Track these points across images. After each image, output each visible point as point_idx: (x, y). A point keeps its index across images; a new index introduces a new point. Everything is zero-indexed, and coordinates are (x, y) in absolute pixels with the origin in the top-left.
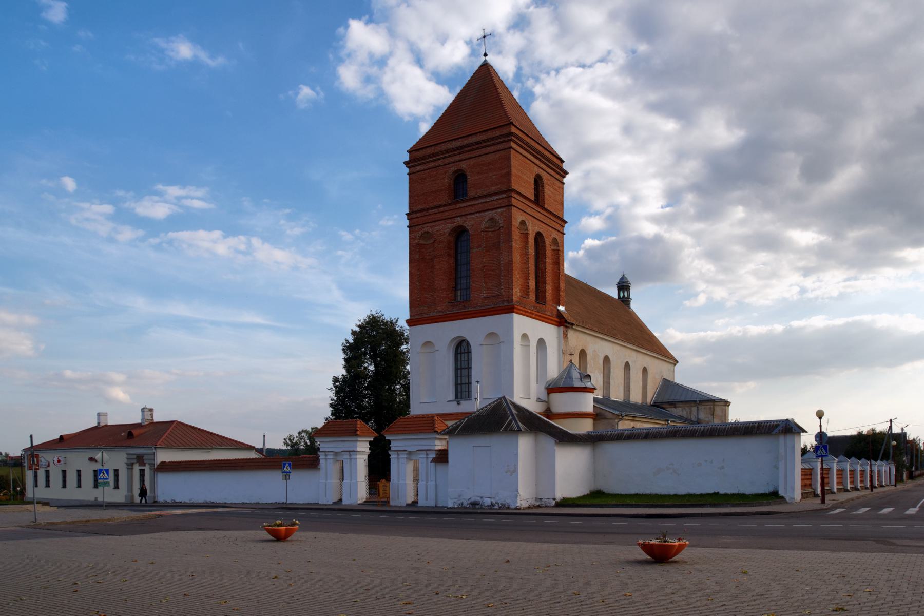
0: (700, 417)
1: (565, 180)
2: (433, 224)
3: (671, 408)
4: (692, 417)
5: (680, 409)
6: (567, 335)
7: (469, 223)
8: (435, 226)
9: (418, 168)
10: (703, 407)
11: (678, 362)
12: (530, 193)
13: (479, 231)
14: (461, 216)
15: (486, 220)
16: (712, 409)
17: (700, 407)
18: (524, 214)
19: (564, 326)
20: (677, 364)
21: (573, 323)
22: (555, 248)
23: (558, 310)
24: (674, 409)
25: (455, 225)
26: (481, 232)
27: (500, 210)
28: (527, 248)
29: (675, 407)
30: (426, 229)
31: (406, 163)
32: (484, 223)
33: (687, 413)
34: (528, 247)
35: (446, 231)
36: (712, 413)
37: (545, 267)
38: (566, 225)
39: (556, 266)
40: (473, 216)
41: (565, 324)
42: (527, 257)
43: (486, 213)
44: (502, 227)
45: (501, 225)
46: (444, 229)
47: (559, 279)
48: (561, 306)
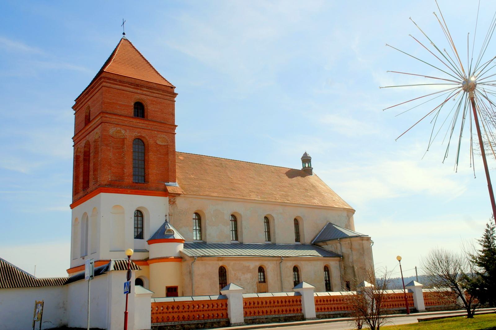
0: (343, 252)
1: (175, 99)
3: (324, 245)
4: (338, 251)
5: (330, 245)
6: (174, 203)
9: (77, 110)
10: (344, 243)
11: (355, 211)
12: (131, 112)
16: (350, 244)
17: (342, 243)
18: (120, 126)
19: (169, 196)
20: (355, 213)
21: (180, 193)
22: (166, 144)
23: (165, 185)
24: (327, 246)
28: (123, 148)
29: (327, 245)
31: (73, 108)
33: (335, 249)
34: (124, 147)
36: (350, 247)
37: (148, 158)
38: (177, 128)
39: (166, 156)
41: (169, 195)
42: (124, 153)
46: (83, 143)
47: (168, 165)
48: (170, 183)
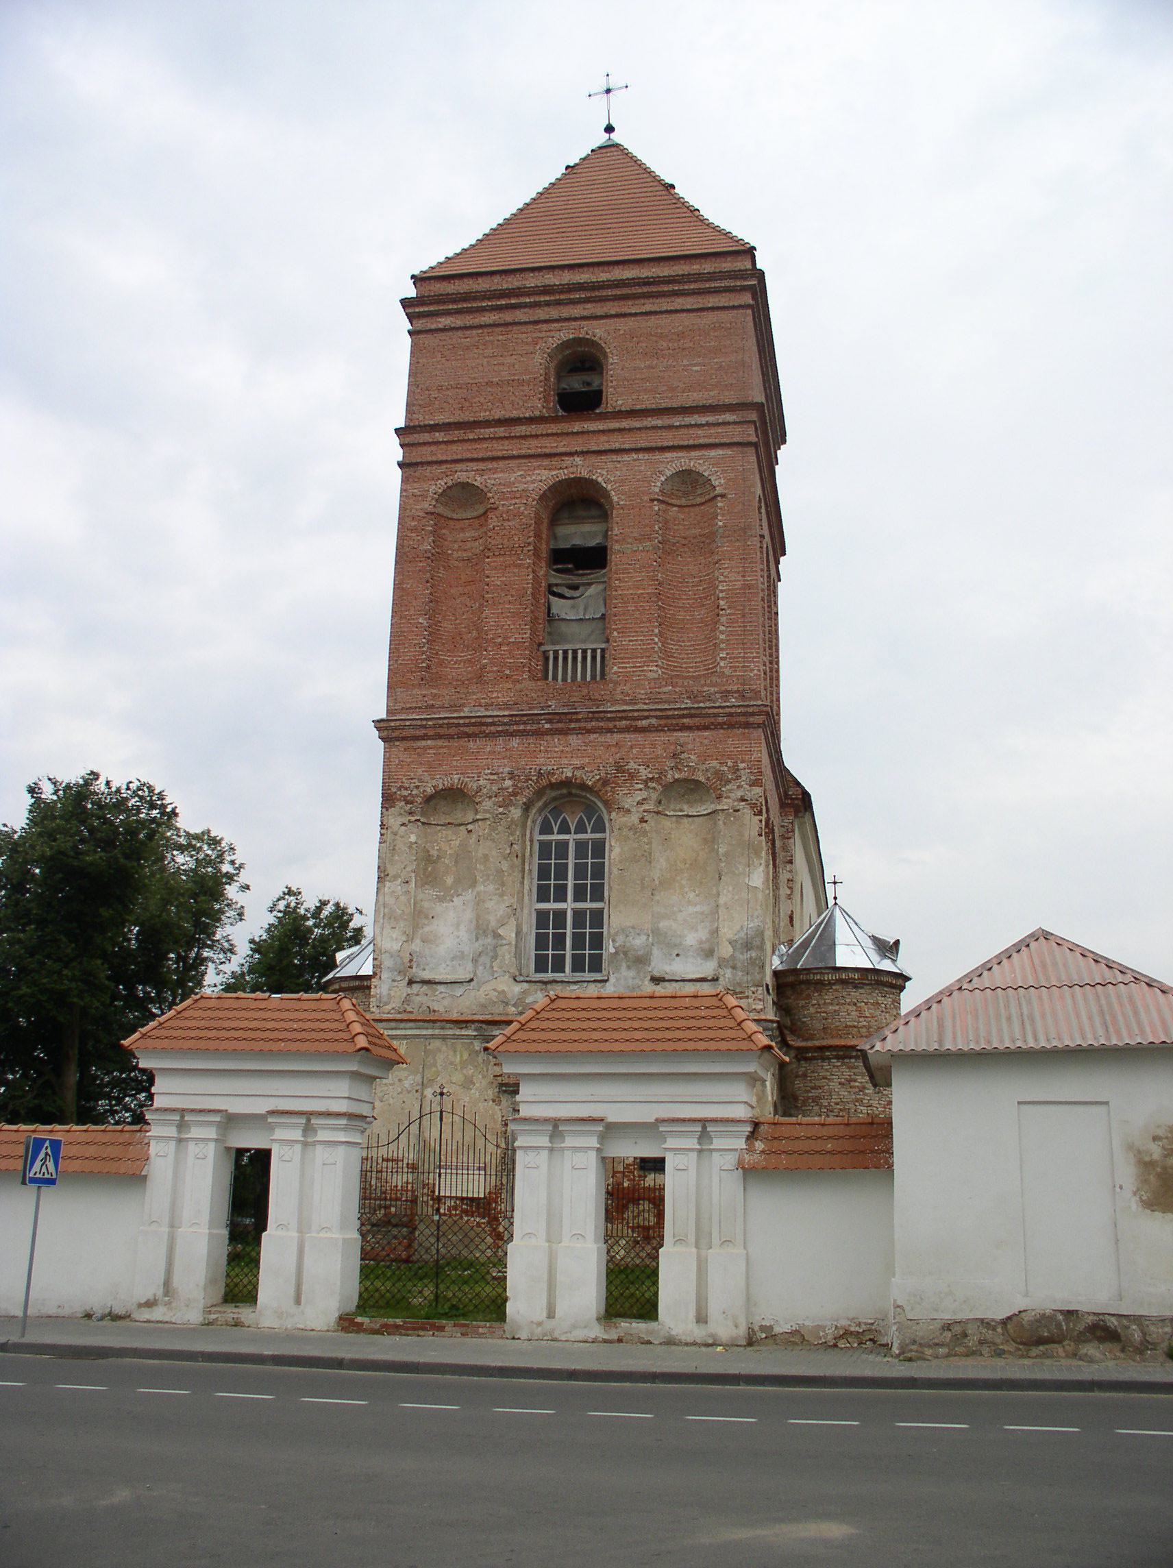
2: (490, 465)
7: (606, 474)
8: (495, 471)
13: (646, 498)
14: (583, 453)
15: (668, 473)
25: (562, 475)
26: (652, 500)
27: (713, 453)
30: (462, 477)
32: (663, 479)
35: (531, 487)
40: (626, 458)
43: (669, 455)
44: (723, 496)
45: (719, 490)
